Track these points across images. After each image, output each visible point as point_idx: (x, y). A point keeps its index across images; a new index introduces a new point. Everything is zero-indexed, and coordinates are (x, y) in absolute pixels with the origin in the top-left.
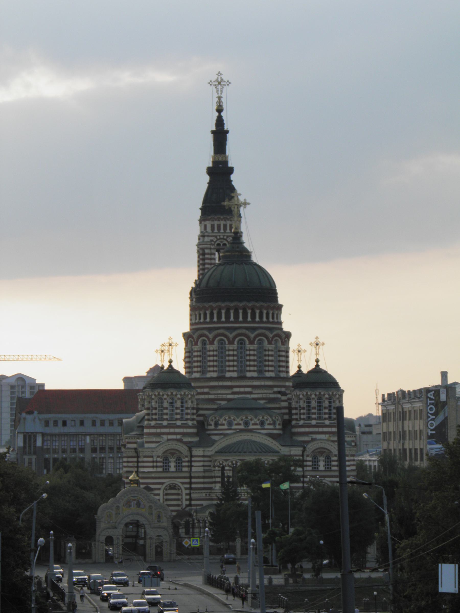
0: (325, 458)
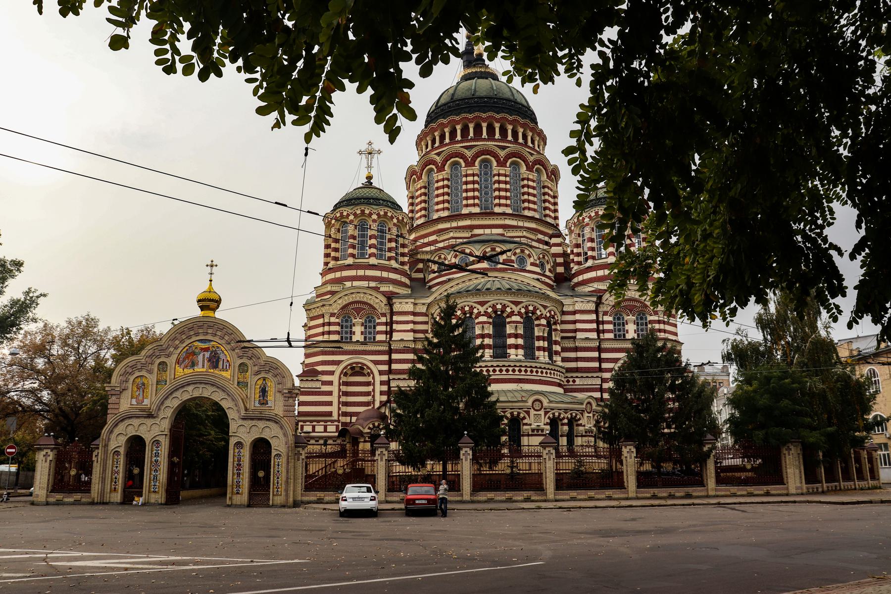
0: (637, 318)
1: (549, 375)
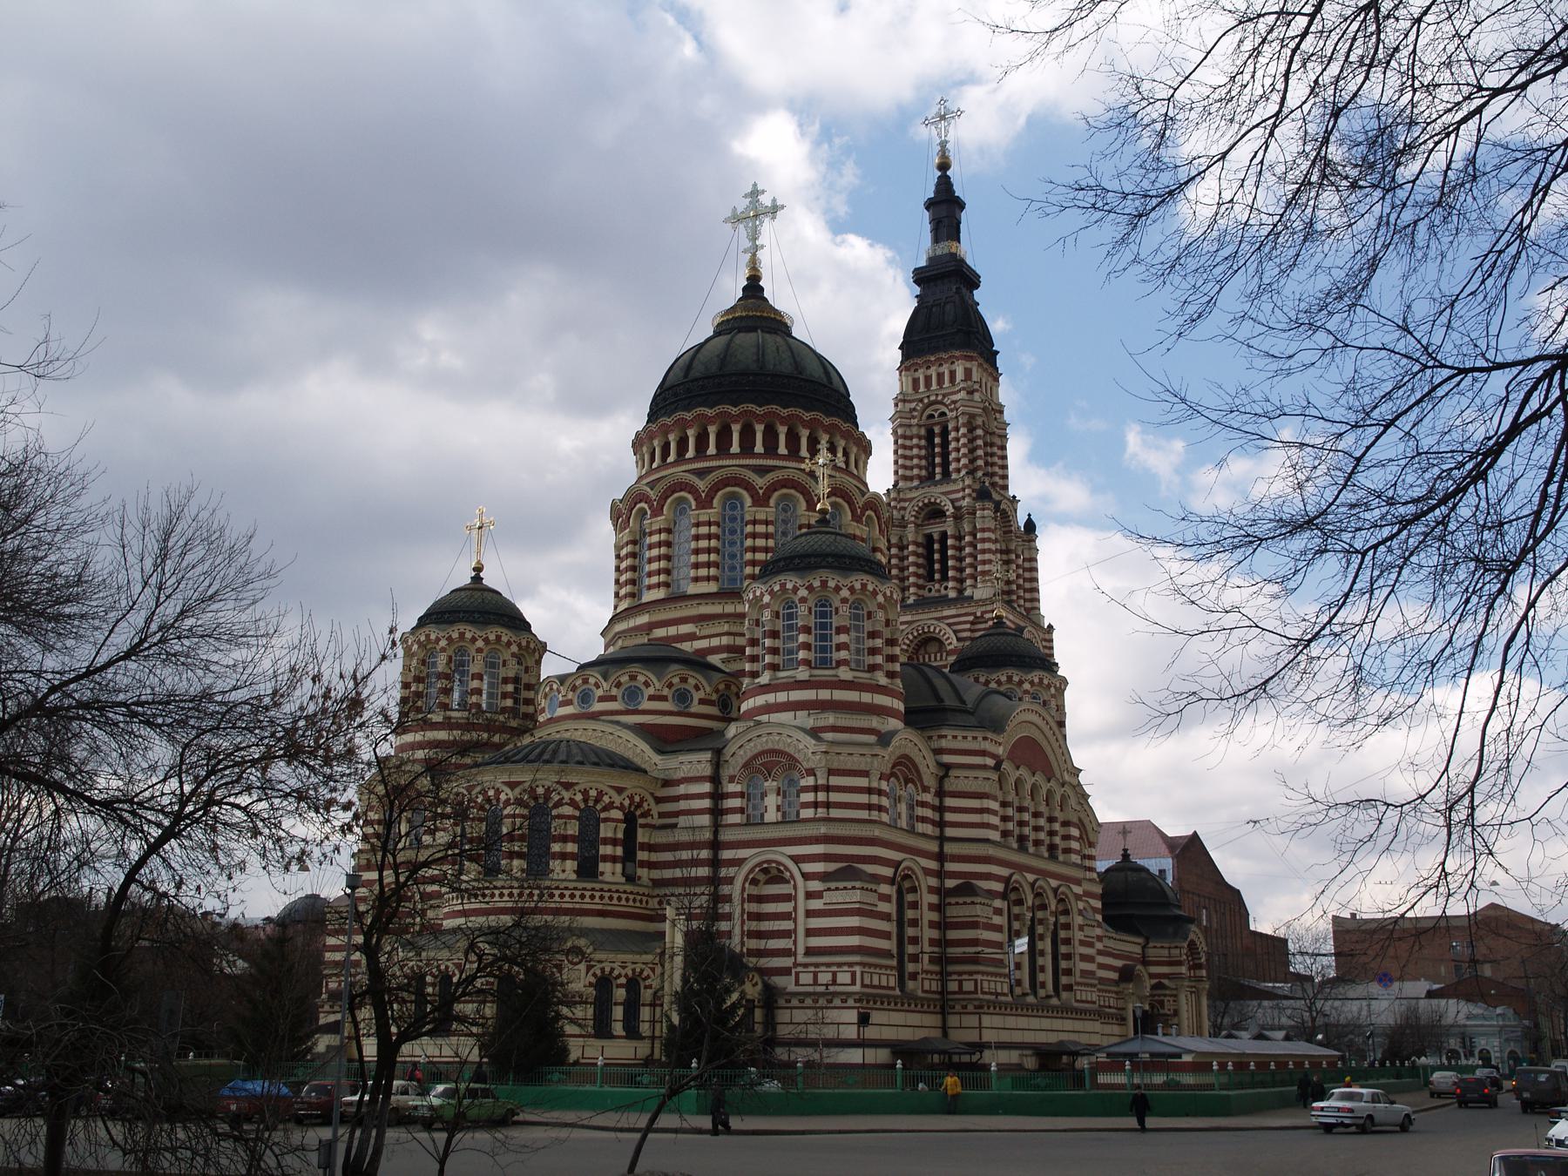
1: (638, 904)
